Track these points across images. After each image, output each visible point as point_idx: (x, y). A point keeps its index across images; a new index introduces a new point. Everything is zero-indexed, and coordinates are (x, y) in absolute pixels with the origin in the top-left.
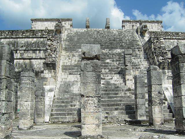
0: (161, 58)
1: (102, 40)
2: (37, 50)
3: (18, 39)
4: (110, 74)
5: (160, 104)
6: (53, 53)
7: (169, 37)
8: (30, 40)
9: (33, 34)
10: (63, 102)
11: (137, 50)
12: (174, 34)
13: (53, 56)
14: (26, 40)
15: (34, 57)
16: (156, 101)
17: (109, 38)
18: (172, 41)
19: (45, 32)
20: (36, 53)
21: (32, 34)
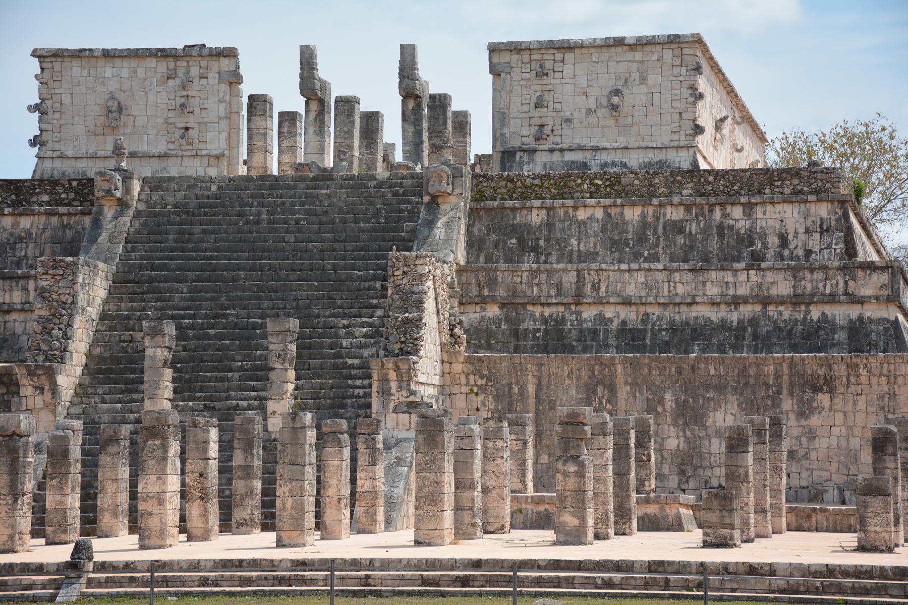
2: (27, 277)
5: (202, 498)
6: (55, 324)
9: (17, 195)
12: (600, 182)
13: (55, 332)
15: (19, 307)
16: (194, 492)
18: (581, 215)
20: (25, 289)
21: (13, 197)
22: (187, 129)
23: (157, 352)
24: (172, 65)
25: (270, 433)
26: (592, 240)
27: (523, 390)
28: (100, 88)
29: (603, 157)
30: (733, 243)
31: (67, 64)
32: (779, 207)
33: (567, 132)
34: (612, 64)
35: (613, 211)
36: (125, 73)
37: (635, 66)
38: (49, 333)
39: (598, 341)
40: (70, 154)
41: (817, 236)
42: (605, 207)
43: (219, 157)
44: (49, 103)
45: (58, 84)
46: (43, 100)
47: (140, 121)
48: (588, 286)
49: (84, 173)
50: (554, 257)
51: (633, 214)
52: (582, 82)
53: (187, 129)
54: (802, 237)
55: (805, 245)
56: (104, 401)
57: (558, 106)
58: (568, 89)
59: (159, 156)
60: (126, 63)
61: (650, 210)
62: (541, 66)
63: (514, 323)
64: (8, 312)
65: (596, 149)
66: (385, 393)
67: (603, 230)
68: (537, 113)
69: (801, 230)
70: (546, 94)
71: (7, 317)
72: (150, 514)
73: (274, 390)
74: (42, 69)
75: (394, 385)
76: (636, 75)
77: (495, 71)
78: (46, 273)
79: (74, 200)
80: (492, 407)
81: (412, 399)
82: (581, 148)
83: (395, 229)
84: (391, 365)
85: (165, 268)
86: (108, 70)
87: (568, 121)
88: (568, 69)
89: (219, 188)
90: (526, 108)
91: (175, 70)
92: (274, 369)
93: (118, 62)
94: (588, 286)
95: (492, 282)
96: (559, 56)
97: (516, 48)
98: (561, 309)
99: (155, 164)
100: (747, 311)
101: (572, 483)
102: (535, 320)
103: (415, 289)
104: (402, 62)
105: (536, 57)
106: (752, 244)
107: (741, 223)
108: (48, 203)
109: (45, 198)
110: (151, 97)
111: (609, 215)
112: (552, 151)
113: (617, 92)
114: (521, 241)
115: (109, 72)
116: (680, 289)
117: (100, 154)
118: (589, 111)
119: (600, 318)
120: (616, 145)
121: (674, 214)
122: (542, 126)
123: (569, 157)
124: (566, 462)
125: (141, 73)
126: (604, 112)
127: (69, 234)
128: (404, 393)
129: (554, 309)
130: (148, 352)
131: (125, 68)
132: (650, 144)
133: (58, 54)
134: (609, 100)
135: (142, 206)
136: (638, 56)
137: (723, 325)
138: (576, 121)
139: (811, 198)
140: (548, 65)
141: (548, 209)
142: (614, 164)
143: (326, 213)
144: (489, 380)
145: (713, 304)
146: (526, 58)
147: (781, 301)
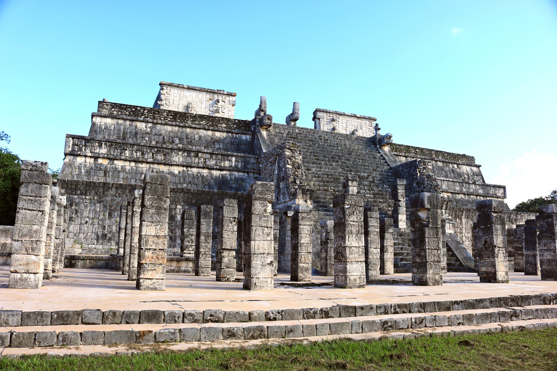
25: (401, 229)
76: (359, 127)
79: (236, 128)
92: (400, 201)
93: (192, 91)
109: (224, 125)
131: (193, 94)
136: (360, 121)
146: (328, 114)
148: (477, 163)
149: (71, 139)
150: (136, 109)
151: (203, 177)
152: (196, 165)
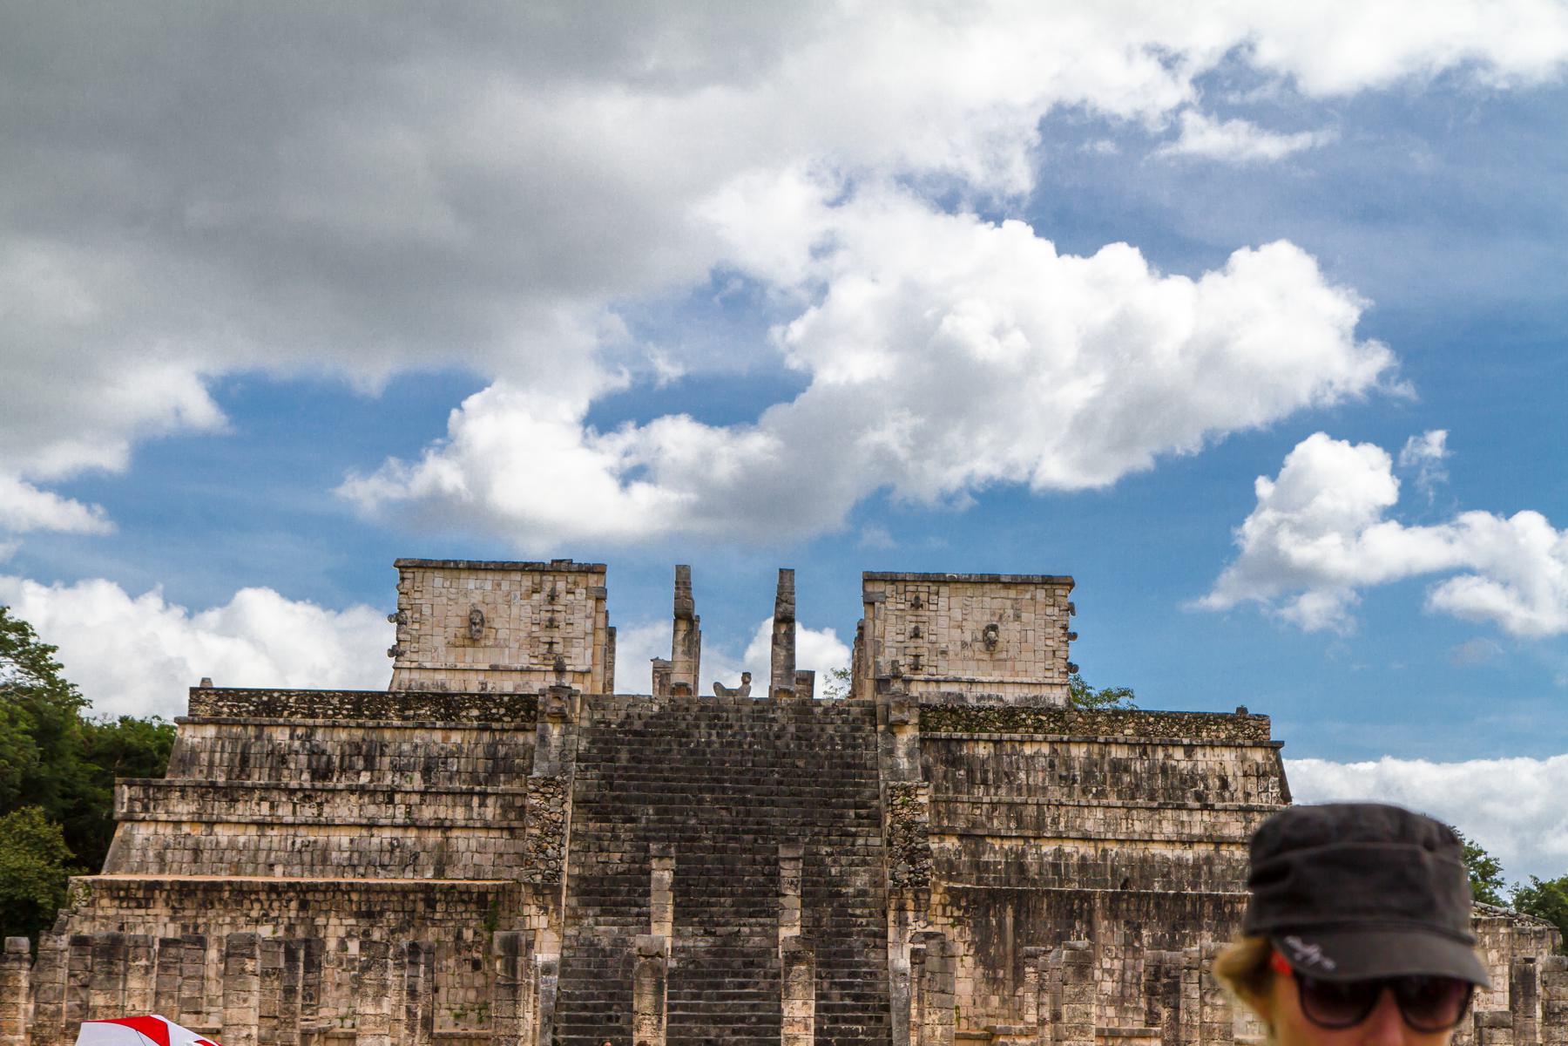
0: (903, 866)
1: (723, 763)
2: (471, 793)
3: (387, 735)
4: (738, 914)
7: (1017, 736)
8: (438, 736)
10: (585, 1008)
11: (852, 813)
13: (550, 851)
14: (419, 736)
15: (463, 823)
17: (756, 753)
18: (1028, 750)
19: (498, 706)
20: (468, 806)
22: (551, 644)
23: (663, 874)
24: (537, 578)
26: (1041, 775)
27: (1001, 924)
28: (462, 600)
29: (979, 690)
30: (1176, 783)
31: (429, 574)
32: (1217, 751)
33: (942, 664)
34: (987, 599)
35: (1058, 747)
36: (488, 586)
37: (1009, 603)
38: (544, 852)
39: (1059, 874)
40: (428, 665)
41: (1254, 779)
42: (1052, 743)
43: (583, 673)
44: (409, 613)
45: (417, 595)
46: (402, 610)
47: (502, 634)
48: (1049, 820)
49: (443, 685)
50: (1003, 791)
51: (1079, 752)
52: (957, 614)
53: (551, 644)
54: (1241, 780)
55: (1244, 787)
56: (597, 924)
57: (933, 638)
58: (943, 621)
59: (522, 671)
60: (490, 576)
61: (1096, 748)
62: (917, 598)
63: (975, 854)
64: (451, 828)
65: (972, 682)
66: (902, 923)
67: (1052, 765)
68: (912, 644)
69: (1240, 774)
70: (921, 626)
71: (449, 834)
72: (796, 1038)
73: (785, 918)
74: (403, 579)
75: (911, 915)
76: (1010, 612)
77: (869, 603)
78: (537, 791)
80: (969, 938)
81: (930, 929)
82: (957, 681)
83: (853, 757)
84: (910, 895)
85: (622, 788)
86: (471, 583)
87: (944, 652)
88: (943, 602)
89: (661, 708)
90: (901, 638)
91: (541, 583)
93: (482, 575)
94: (1049, 820)
95: (952, 814)
96: (934, 588)
97: (892, 579)
98: (1021, 842)
99: (517, 677)
100: (1202, 850)
101: (1219, 1015)
102: (995, 852)
103: (917, 819)
104: (781, 587)
105: (911, 588)
106: (1195, 785)
107: (1183, 765)
108: (478, 718)
109: (475, 712)
110: (515, 611)
111: (1055, 751)
112: (927, 681)
113: (994, 628)
114: (970, 773)
115: (471, 584)
116: (1138, 827)
117: (460, 666)
118: (964, 645)
119: (1059, 853)
120: (991, 679)
121: (1118, 753)
122: (917, 656)
123: (945, 688)
124: (1213, 996)
125: (505, 586)
126: (979, 646)
127: (502, 750)
128: (922, 924)
129: (1014, 842)
130: (655, 875)
131: (488, 581)
132: (1025, 680)
133: (424, 566)
134: (985, 634)
135: (586, 724)
136: (1012, 593)
137: (1179, 864)
138: (951, 653)
139: (1249, 742)
140: (923, 596)
141: (996, 742)
142: (990, 697)
143: (778, 737)
144: (966, 911)
145: (1169, 842)
146: (901, 587)
147: (1231, 842)
148: (1274, 736)
149: (125, 787)
150: (271, 697)
151: (402, 846)
152: (388, 821)
